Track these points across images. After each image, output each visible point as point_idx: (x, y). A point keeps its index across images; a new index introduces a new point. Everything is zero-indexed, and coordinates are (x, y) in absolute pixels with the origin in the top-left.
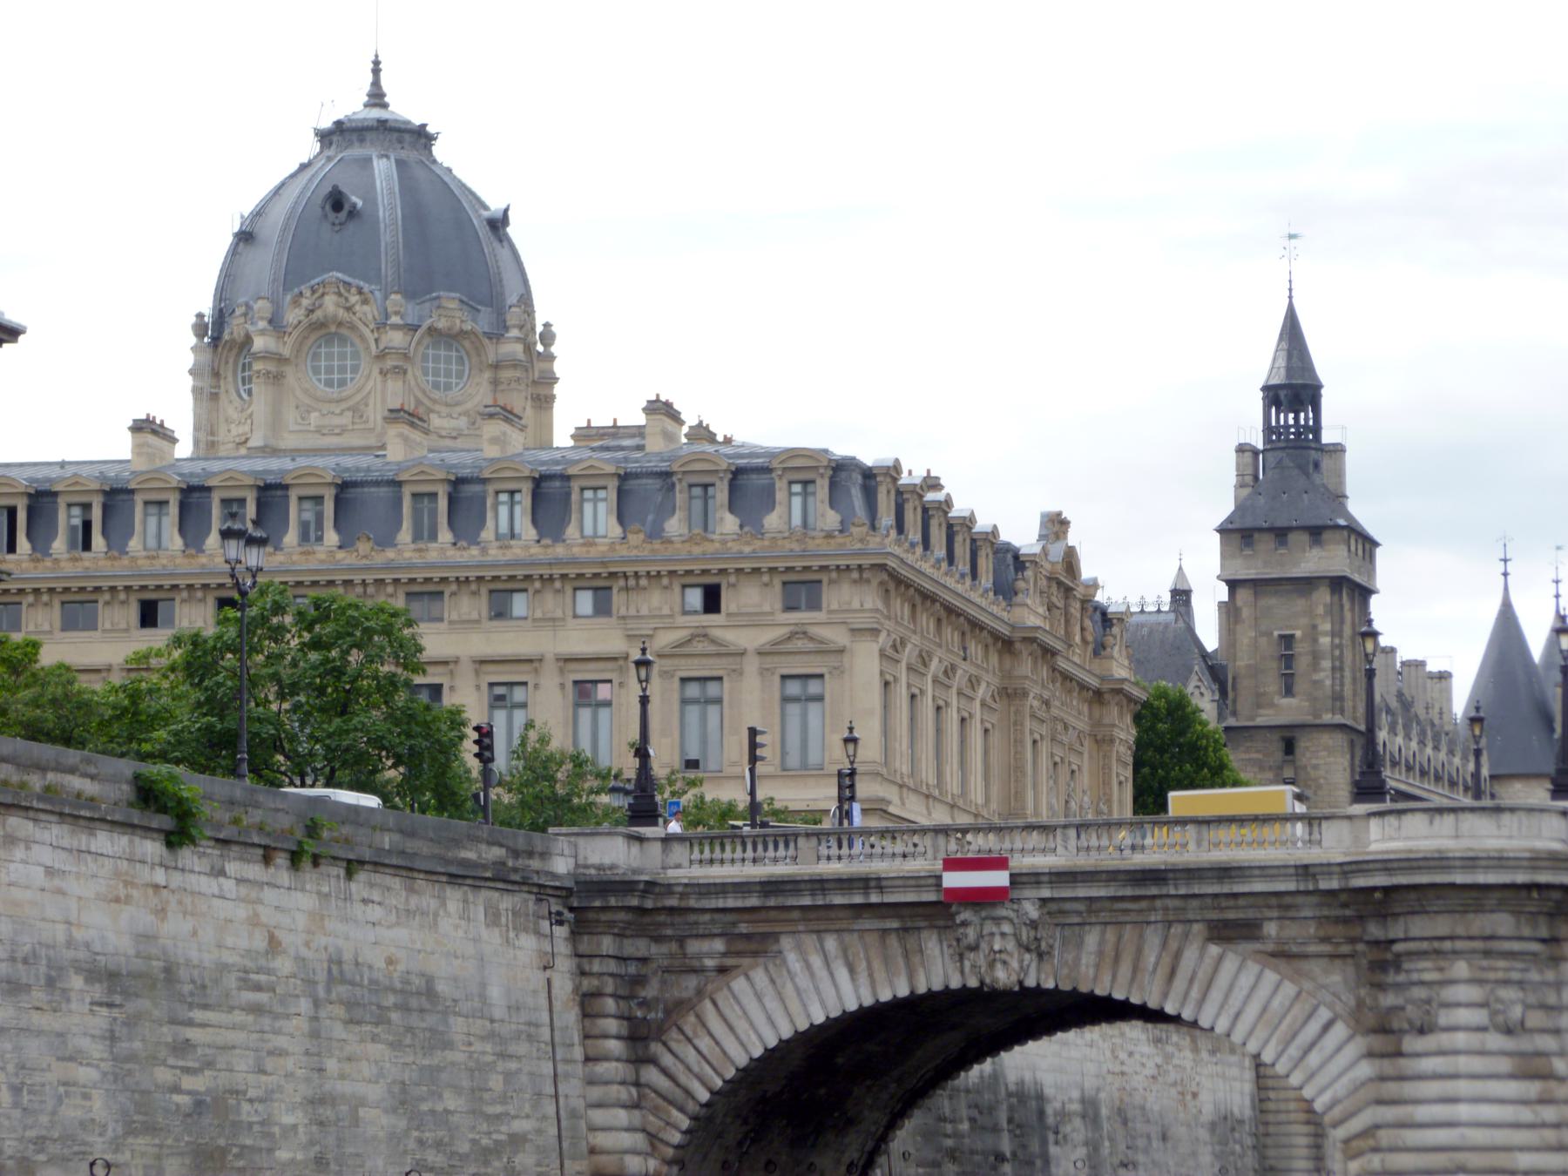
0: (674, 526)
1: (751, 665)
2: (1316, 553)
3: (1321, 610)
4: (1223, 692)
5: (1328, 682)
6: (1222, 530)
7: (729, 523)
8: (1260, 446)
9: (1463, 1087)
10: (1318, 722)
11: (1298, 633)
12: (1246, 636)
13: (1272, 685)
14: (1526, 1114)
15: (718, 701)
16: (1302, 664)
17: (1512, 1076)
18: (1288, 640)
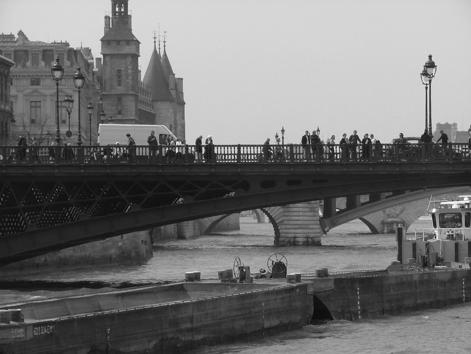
0: (29, 64)
1: (48, 99)
2: (128, 47)
3: (129, 63)
4: (101, 84)
5: (131, 83)
6: (101, 40)
7: (43, 64)
8: (111, 17)
9: (301, 213)
10: (128, 93)
11: (122, 69)
12: (108, 70)
13: (115, 83)
14: (311, 218)
15: (40, 107)
16: (123, 77)
17: (309, 212)
18: (119, 71)
